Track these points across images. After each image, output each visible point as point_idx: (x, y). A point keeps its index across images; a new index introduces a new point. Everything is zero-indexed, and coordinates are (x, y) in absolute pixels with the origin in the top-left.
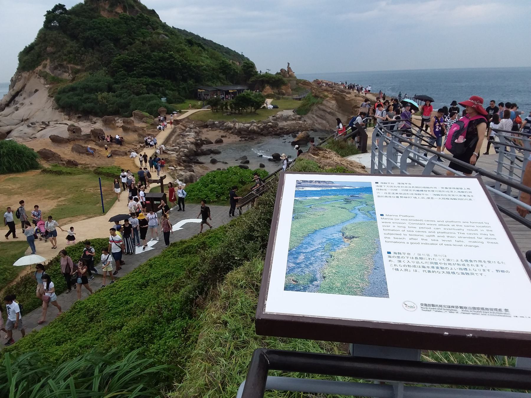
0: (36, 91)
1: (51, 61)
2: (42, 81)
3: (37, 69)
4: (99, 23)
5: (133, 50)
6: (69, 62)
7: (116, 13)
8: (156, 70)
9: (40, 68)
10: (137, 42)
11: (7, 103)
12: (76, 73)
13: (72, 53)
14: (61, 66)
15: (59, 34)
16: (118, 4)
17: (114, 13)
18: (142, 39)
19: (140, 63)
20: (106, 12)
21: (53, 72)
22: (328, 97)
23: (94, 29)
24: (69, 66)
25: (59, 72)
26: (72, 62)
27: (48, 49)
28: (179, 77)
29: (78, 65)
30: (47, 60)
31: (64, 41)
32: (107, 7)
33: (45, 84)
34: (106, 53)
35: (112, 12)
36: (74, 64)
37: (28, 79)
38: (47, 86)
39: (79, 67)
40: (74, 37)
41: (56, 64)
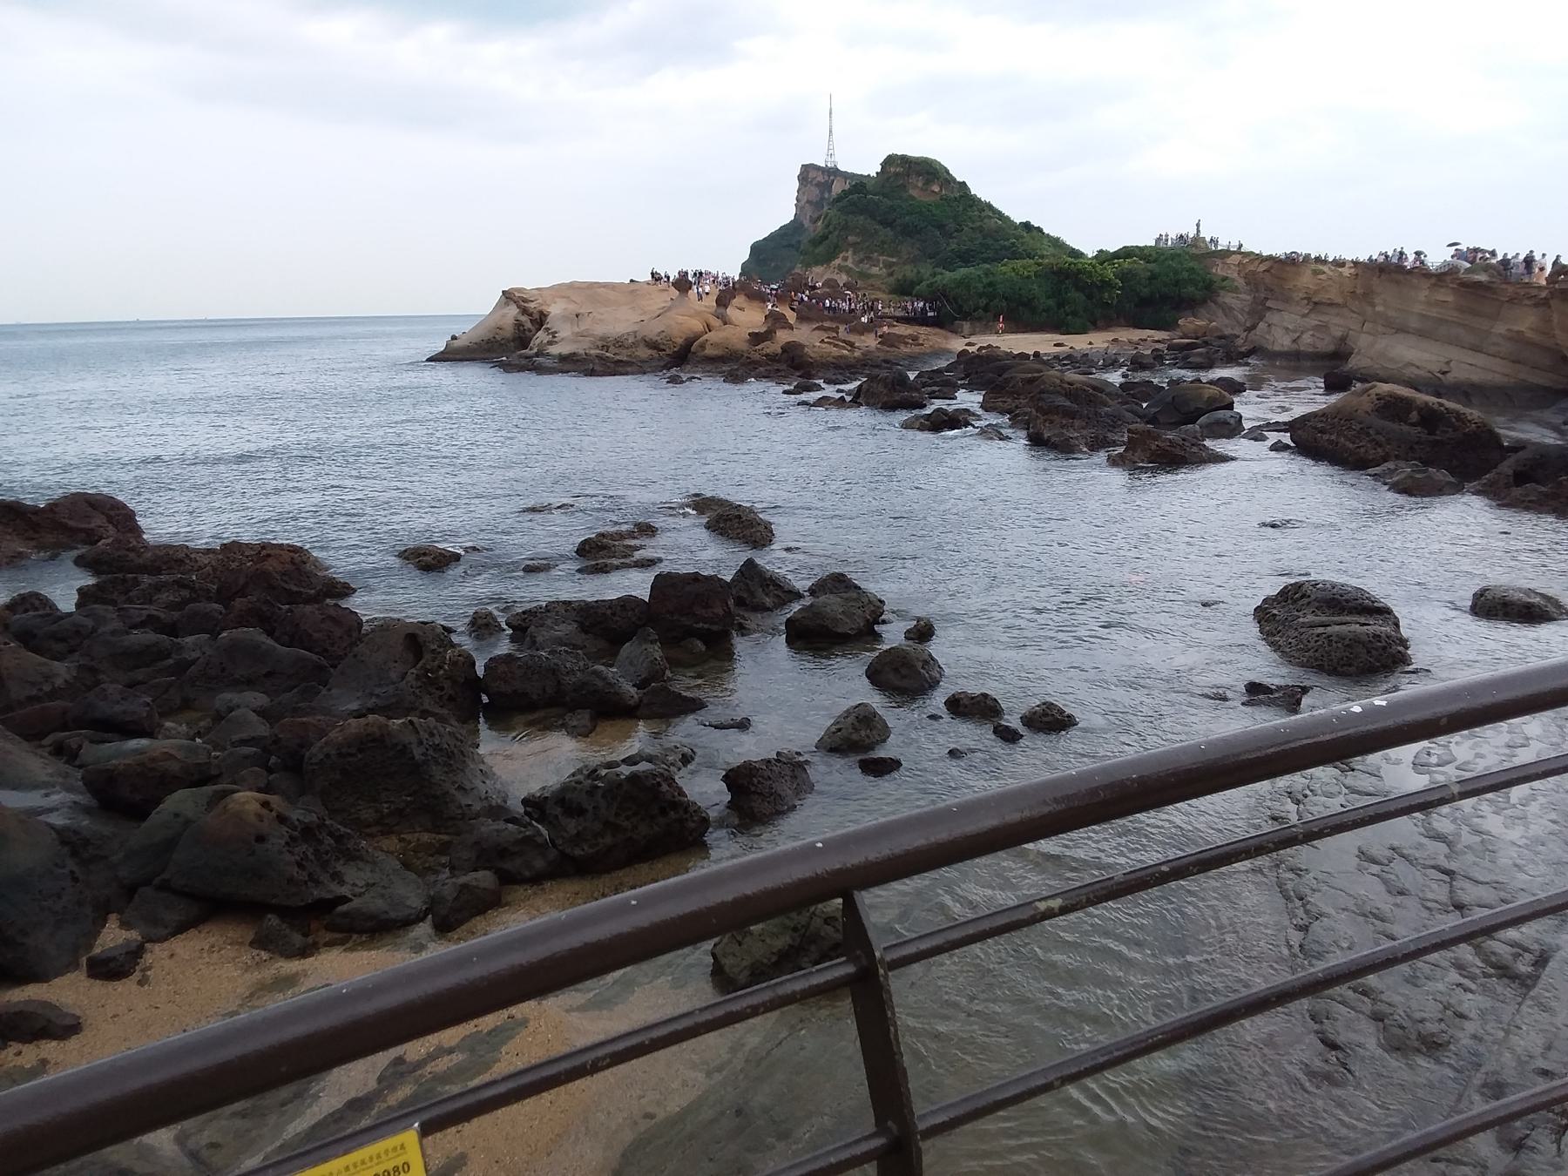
5: (964, 238)
6: (882, 254)
9: (837, 262)
10: (966, 228)
12: (890, 267)
14: (869, 258)
15: (866, 219)
18: (971, 225)
21: (857, 266)
24: (881, 258)
27: (849, 238)
29: (893, 257)
32: (920, 184)
36: (888, 256)
40: (886, 223)
41: (862, 256)
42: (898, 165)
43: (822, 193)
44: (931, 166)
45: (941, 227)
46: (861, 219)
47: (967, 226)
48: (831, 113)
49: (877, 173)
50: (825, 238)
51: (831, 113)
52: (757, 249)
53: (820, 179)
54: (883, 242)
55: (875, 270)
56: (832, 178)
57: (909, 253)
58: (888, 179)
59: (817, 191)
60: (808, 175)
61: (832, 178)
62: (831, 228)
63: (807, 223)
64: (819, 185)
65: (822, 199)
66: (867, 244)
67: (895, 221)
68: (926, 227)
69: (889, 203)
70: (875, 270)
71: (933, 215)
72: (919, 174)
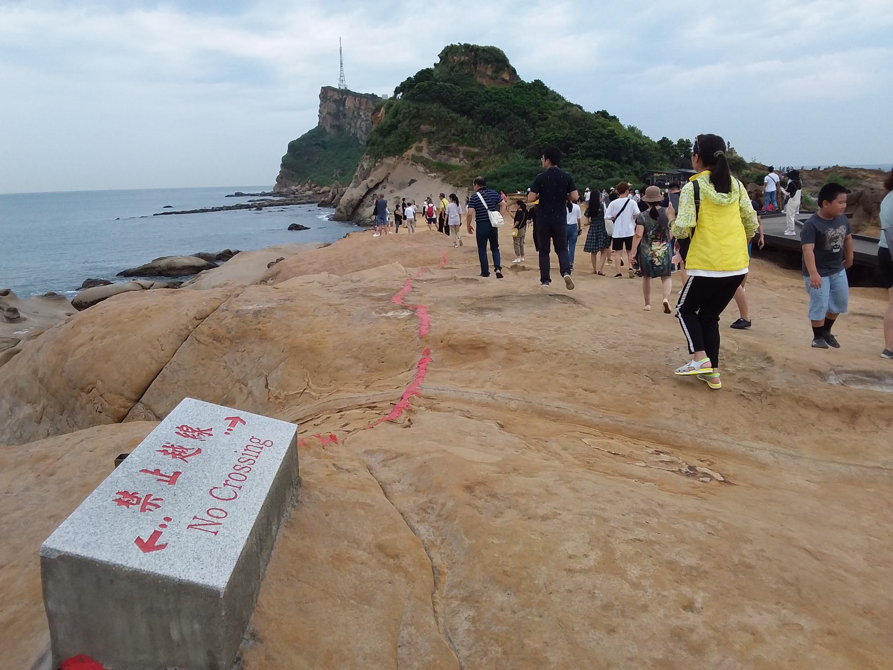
0: (413, 181)
1: (430, 143)
2: (421, 168)
3: (406, 153)
4: (496, 94)
6: (462, 144)
7: (503, 80)
8: (602, 150)
9: (411, 152)
11: (361, 198)
12: (473, 158)
13: (466, 132)
14: (446, 149)
16: (506, 68)
17: (500, 81)
19: (577, 142)
20: (488, 78)
21: (435, 158)
22: (869, 177)
23: (490, 101)
24: (462, 148)
25: (446, 157)
26: (466, 144)
27: (422, 127)
28: (624, 158)
29: (474, 147)
30: (421, 141)
31: (451, 117)
32: (489, 73)
33: (427, 173)
34: (518, 131)
35: (497, 78)
36: (469, 145)
37: (394, 167)
38: (433, 175)
39: (476, 150)
40: (463, 112)
42: (462, 54)
43: (338, 107)
44: (499, 54)
45: (524, 115)
46: (434, 107)
47: (550, 114)
48: (341, 51)
49: (435, 64)
50: (393, 127)
51: (341, 51)
52: (292, 146)
53: (336, 97)
54: (463, 131)
55: (455, 161)
56: (344, 96)
57: (492, 143)
58: (452, 69)
59: (333, 106)
60: (326, 93)
61: (344, 96)
62: (400, 117)
63: (328, 129)
64: (335, 101)
65: (339, 111)
66: (444, 133)
67: (473, 108)
68: (510, 114)
69: (465, 90)
70: (455, 161)
71: (514, 102)
72: (487, 62)
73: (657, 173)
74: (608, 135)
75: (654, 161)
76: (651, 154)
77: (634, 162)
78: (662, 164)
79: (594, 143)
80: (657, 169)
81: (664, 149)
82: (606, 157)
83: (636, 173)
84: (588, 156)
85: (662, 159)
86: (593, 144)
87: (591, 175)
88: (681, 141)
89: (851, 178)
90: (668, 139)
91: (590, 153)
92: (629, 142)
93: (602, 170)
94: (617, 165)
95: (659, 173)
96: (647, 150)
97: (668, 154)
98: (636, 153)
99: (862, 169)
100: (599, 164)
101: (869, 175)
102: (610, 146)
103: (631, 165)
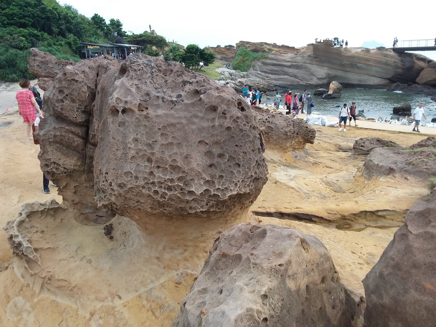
22: (273, 50)
28: (55, 30)
73: (90, 45)
74: (35, 4)
75: (88, 35)
76: (84, 28)
77: (67, 34)
78: (96, 38)
79: (16, 10)
80: (91, 42)
81: (97, 25)
82: (33, 26)
83: (69, 44)
84: (12, 24)
85: (97, 34)
86: (15, 11)
87: (9, 44)
88: (112, 21)
89: (258, 52)
90: (99, 16)
91: (13, 21)
92: (59, 15)
93: (23, 39)
94: (46, 35)
95: (92, 46)
96: (80, 23)
97: (103, 30)
98: (68, 25)
99: (266, 44)
100: (21, 33)
101: (273, 49)
102: (36, 15)
103: (64, 36)
